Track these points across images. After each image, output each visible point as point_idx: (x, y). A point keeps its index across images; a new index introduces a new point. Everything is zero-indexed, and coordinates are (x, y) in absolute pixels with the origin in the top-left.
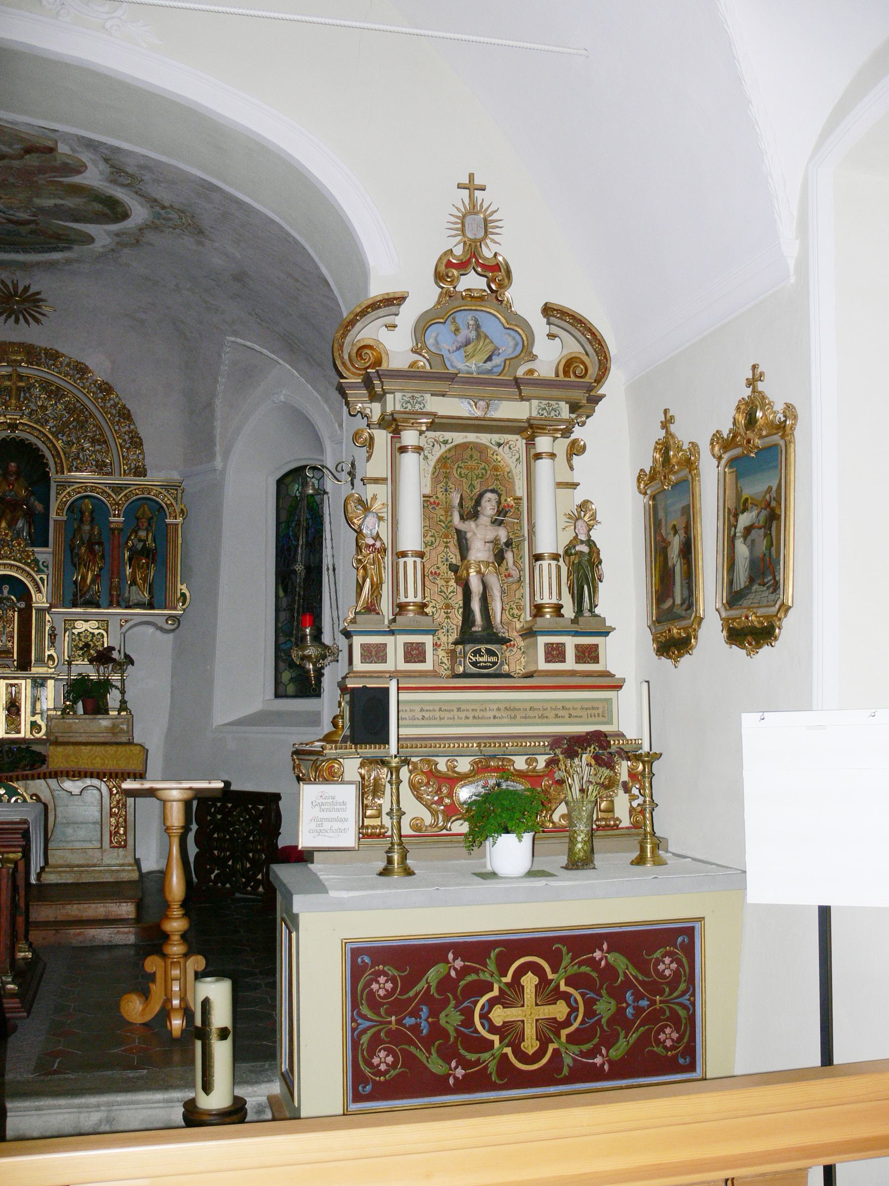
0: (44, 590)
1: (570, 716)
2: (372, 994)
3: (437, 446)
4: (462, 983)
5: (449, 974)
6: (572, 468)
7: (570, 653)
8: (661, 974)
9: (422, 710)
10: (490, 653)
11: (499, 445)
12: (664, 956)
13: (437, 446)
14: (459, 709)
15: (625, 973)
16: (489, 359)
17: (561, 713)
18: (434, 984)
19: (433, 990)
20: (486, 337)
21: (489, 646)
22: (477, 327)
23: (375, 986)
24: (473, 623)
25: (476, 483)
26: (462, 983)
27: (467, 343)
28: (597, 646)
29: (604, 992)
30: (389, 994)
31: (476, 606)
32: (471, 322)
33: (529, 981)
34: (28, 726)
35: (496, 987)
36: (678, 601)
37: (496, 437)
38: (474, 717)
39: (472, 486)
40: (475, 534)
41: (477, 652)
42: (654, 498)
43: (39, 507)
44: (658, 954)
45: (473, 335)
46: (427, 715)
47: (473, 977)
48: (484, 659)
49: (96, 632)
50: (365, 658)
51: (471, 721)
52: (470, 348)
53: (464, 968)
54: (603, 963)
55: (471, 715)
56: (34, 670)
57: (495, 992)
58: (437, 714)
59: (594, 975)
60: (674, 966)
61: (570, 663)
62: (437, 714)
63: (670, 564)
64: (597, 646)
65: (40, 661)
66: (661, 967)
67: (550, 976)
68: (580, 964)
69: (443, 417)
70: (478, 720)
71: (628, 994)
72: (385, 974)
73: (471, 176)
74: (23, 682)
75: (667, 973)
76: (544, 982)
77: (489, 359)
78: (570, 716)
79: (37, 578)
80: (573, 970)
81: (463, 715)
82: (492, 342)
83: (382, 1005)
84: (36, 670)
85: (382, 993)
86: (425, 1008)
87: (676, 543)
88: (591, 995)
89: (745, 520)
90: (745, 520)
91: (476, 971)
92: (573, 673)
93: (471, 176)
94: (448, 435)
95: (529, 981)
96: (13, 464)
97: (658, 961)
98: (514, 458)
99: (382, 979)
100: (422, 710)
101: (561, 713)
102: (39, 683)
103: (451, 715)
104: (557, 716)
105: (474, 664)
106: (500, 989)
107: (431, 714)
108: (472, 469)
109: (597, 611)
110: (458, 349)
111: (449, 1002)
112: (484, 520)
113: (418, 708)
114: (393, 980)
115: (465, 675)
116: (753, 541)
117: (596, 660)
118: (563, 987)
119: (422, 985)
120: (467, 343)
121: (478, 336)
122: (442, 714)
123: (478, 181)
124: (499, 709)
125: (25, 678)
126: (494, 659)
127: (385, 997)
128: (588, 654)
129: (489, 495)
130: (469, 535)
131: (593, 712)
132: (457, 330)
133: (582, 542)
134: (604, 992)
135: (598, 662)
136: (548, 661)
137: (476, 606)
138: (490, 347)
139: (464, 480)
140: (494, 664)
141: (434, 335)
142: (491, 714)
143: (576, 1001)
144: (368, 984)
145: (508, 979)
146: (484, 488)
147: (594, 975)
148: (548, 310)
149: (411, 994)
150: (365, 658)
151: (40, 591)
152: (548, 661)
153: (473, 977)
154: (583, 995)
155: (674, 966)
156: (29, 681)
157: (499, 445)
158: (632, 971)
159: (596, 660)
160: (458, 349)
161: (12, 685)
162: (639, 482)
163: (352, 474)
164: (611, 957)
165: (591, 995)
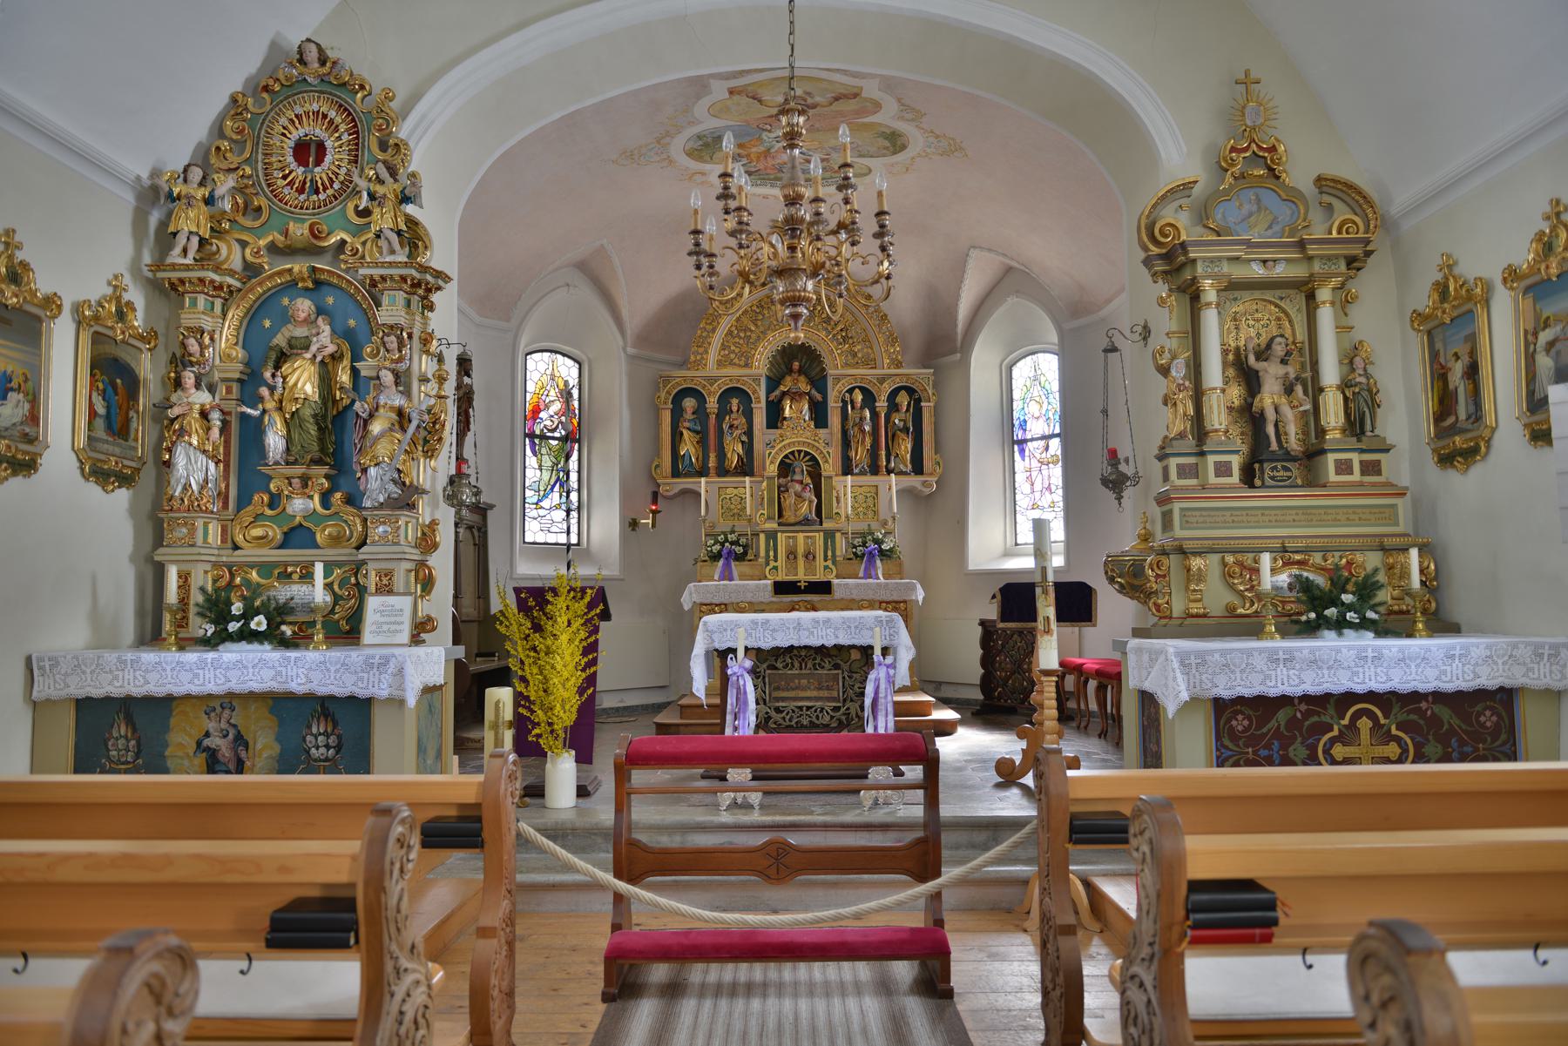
0: (830, 461)
1: (1360, 519)
2: (1232, 728)
4: (1307, 723)
5: (1295, 716)
6: (1346, 314)
7: (1356, 467)
8: (1483, 725)
9: (1232, 515)
10: (1286, 469)
11: (1281, 299)
12: (1485, 709)
13: (1228, 303)
14: (1263, 514)
15: (1449, 723)
16: (1270, 227)
17: (1352, 517)
18: (1283, 723)
19: (1282, 728)
20: (1266, 209)
21: (1285, 464)
22: (1258, 201)
23: (1234, 723)
24: (1269, 445)
25: (1263, 331)
26: (1307, 723)
27: (1250, 215)
28: (1379, 461)
29: (1431, 737)
30: (1246, 730)
31: (1271, 430)
32: (1253, 198)
33: (1365, 724)
34: (822, 569)
35: (1336, 728)
36: (1462, 415)
37: (1279, 293)
38: (1276, 521)
39: (1259, 335)
40: (1266, 371)
41: (1274, 469)
42: (1429, 333)
43: (819, 397)
44: (1479, 708)
45: (1255, 208)
47: (1315, 719)
48: (1281, 473)
49: (868, 495)
50: (1180, 476)
51: (1274, 524)
52: (1252, 219)
53: (1306, 710)
54: (1429, 713)
55: (1274, 518)
56: (825, 525)
57: (1335, 732)
58: (1245, 518)
59: (1422, 722)
60: (1494, 718)
61: (1356, 476)
62: (1245, 518)
63: (1451, 387)
64: (1379, 461)
65: (830, 517)
66: (1482, 719)
67: (1383, 721)
68: (1409, 712)
70: (1279, 523)
71: (1453, 740)
72: (1242, 713)
73: (1247, 73)
74: (817, 534)
75: (1488, 724)
76: (1376, 724)
77: (1270, 227)
78: (1360, 519)
79: (825, 452)
80: (1402, 717)
82: (1271, 213)
83: (1241, 738)
84: (827, 525)
85: (1240, 728)
86: (1276, 743)
87: (1457, 370)
88: (1419, 739)
89: (1545, 337)
90: (1545, 337)
91: (1319, 714)
92: (1361, 484)
93: (1247, 73)
95: (1365, 724)
96: (797, 363)
97: (1479, 714)
98: (1295, 309)
99: (1240, 717)
100: (1232, 515)
101: (1352, 517)
102: (830, 535)
103: (1256, 519)
104: (1348, 519)
105: (1272, 478)
106: (1339, 729)
107: (1240, 518)
108: (1258, 320)
109: (1377, 432)
110: (1243, 220)
111: (1296, 739)
114: (1249, 718)
115: (1263, 486)
116: (1558, 353)
117: (1379, 473)
118: (1394, 731)
119: (1273, 724)
120: (1250, 215)
121: (1259, 209)
122: (1250, 518)
123: (1253, 75)
124: (1297, 514)
125: (818, 531)
126: (1289, 474)
127: (1243, 732)
128: (1371, 468)
130: (1261, 374)
131: (1381, 515)
133: (1360, 375)
134: (1431, 737)
135: (1381, 475)
136: (1337, 473)
138: (1270, 218)
139: (1252, 330)
141: (1221, 210)
142: (1291, 518)
143: (1406, 742)
144: (1229, 721)
145: (1346, 722)
146: (1270, 336)
147: (1422, 722)
148: (1320, 180)
149: (1264, 730)
150: (1180, 476)
151: (827, 461)
152: (1337, 473)
153: (1315, 719)
154: (1412, 739)
155: (1494, 718)
156: (822, 534)
158: (1456, 722)
159: (1379, 473)
160: (1243, 220)
161: (808, 537)
163: (1146, 333)
164: (1437, 709)
165: (1419, 739)
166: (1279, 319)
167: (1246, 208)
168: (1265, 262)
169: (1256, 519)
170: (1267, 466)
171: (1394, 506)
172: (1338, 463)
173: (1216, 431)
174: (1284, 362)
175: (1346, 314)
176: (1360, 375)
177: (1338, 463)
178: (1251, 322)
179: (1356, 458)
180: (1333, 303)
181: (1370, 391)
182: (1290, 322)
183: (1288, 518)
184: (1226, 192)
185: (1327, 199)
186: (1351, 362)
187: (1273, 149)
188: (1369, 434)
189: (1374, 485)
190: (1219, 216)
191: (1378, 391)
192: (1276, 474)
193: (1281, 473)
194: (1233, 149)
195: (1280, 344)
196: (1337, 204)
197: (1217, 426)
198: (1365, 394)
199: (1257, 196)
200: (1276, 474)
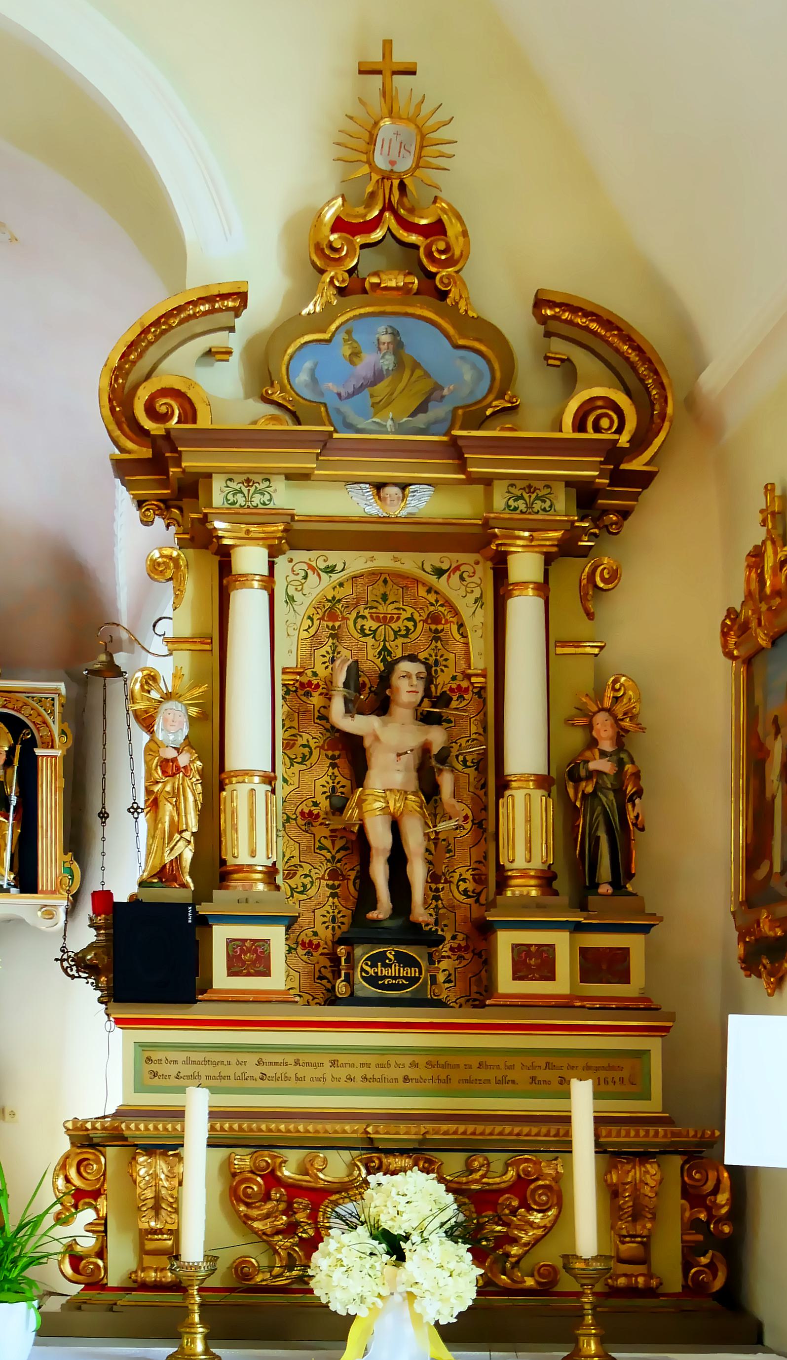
3: (312, 577)
9: (260, 1062)
10: (405, 960)
11: (439, 572)
13: (312, 577)
14: (334, 1063)
16: (422, 408)
20: (416, 365)
21: (403, 949)
24: (373, 904)
27: (378, 377)
31: (380, 872)
32: (386, 338)
37: (433, 559)
38: (365, 1078)
40: (377, 738)
41: (380, 958)
45: (388, 362)
46: (270, 1071)
48: (394, 970)
52: (382, 388)
55: (358, 1073)
58: (291, 1071)
62: (291, 1071)
64: (625, 952)
69: (310, 519)
77: (422, 408)
81: (342, 1073)
82: (427, 375)
94: (335, 557)
98: (471, 598)
100: (260, 1062)
101: (542, 1075)
103: (318, 1073)
104: (533, 1079)
105: (373, 981)
107: (279, 1070)
108: (385, 620)
110: (357, 391)
112: (402, 713)
113: (252, 1059)
115: (353, 1000)
117: (624, 977)
121: (399, 364)
122: (301, 1071)
124: (414, 1065)
126: (412, 972)
129: (405, 666)
130: (367, 743)
131: (610, 1074)
132: (355, 355)
133: (603, 754)
135: (628, 982)
136: (518, 975)
137: (380, 872)
138: (424, 387)
139: (369, 640)
140: (413, 980)
141: (308, 365)
152: (518, 975)
157: (439, 572)
160: (357, 391)
162: (725, 635)
166: (435, 619)
167: (369, 361)
168: (379, 487)
169: (318, 1073)
170: (362, 953)
171: (642, 1055)
172: (521, 953)
173: (250, 868)
174: (427, 719)
175: (590, 615)
176: (603, 754)
177: (521, 953)
178: (370, 624)
179: (561, 941)
180: (543, 588)
181: (619, 791)
182: (461, 625)
183: (387, 1072)
184: (317, 322)
185: (560, 347)
186: (590, 727)
187: (437, 229)
188: (605, 889)
189: (606, 1006)
190: (301, 378)
191: (639, 793)
192: (380, 970)
193: (394, 970)
194: (339, 225)
195: (408, 676)
196: (582, 359)
197: (244, 859)
198: (608, 799)
199: (395, 334)
200: (380, 970)
